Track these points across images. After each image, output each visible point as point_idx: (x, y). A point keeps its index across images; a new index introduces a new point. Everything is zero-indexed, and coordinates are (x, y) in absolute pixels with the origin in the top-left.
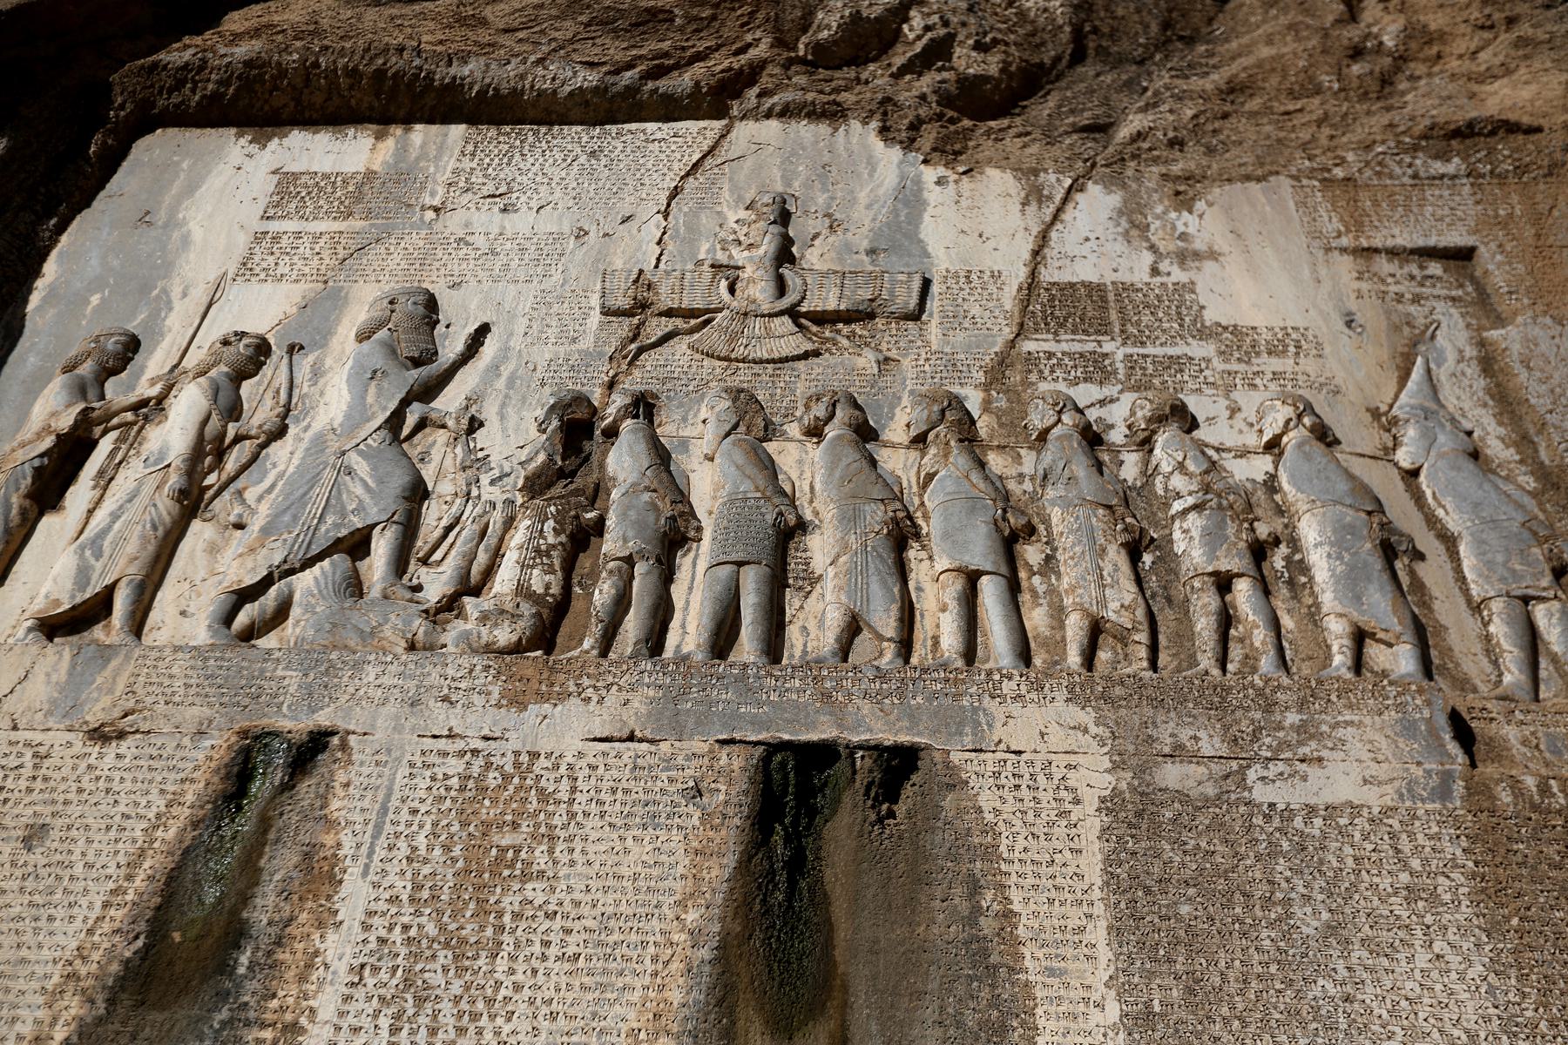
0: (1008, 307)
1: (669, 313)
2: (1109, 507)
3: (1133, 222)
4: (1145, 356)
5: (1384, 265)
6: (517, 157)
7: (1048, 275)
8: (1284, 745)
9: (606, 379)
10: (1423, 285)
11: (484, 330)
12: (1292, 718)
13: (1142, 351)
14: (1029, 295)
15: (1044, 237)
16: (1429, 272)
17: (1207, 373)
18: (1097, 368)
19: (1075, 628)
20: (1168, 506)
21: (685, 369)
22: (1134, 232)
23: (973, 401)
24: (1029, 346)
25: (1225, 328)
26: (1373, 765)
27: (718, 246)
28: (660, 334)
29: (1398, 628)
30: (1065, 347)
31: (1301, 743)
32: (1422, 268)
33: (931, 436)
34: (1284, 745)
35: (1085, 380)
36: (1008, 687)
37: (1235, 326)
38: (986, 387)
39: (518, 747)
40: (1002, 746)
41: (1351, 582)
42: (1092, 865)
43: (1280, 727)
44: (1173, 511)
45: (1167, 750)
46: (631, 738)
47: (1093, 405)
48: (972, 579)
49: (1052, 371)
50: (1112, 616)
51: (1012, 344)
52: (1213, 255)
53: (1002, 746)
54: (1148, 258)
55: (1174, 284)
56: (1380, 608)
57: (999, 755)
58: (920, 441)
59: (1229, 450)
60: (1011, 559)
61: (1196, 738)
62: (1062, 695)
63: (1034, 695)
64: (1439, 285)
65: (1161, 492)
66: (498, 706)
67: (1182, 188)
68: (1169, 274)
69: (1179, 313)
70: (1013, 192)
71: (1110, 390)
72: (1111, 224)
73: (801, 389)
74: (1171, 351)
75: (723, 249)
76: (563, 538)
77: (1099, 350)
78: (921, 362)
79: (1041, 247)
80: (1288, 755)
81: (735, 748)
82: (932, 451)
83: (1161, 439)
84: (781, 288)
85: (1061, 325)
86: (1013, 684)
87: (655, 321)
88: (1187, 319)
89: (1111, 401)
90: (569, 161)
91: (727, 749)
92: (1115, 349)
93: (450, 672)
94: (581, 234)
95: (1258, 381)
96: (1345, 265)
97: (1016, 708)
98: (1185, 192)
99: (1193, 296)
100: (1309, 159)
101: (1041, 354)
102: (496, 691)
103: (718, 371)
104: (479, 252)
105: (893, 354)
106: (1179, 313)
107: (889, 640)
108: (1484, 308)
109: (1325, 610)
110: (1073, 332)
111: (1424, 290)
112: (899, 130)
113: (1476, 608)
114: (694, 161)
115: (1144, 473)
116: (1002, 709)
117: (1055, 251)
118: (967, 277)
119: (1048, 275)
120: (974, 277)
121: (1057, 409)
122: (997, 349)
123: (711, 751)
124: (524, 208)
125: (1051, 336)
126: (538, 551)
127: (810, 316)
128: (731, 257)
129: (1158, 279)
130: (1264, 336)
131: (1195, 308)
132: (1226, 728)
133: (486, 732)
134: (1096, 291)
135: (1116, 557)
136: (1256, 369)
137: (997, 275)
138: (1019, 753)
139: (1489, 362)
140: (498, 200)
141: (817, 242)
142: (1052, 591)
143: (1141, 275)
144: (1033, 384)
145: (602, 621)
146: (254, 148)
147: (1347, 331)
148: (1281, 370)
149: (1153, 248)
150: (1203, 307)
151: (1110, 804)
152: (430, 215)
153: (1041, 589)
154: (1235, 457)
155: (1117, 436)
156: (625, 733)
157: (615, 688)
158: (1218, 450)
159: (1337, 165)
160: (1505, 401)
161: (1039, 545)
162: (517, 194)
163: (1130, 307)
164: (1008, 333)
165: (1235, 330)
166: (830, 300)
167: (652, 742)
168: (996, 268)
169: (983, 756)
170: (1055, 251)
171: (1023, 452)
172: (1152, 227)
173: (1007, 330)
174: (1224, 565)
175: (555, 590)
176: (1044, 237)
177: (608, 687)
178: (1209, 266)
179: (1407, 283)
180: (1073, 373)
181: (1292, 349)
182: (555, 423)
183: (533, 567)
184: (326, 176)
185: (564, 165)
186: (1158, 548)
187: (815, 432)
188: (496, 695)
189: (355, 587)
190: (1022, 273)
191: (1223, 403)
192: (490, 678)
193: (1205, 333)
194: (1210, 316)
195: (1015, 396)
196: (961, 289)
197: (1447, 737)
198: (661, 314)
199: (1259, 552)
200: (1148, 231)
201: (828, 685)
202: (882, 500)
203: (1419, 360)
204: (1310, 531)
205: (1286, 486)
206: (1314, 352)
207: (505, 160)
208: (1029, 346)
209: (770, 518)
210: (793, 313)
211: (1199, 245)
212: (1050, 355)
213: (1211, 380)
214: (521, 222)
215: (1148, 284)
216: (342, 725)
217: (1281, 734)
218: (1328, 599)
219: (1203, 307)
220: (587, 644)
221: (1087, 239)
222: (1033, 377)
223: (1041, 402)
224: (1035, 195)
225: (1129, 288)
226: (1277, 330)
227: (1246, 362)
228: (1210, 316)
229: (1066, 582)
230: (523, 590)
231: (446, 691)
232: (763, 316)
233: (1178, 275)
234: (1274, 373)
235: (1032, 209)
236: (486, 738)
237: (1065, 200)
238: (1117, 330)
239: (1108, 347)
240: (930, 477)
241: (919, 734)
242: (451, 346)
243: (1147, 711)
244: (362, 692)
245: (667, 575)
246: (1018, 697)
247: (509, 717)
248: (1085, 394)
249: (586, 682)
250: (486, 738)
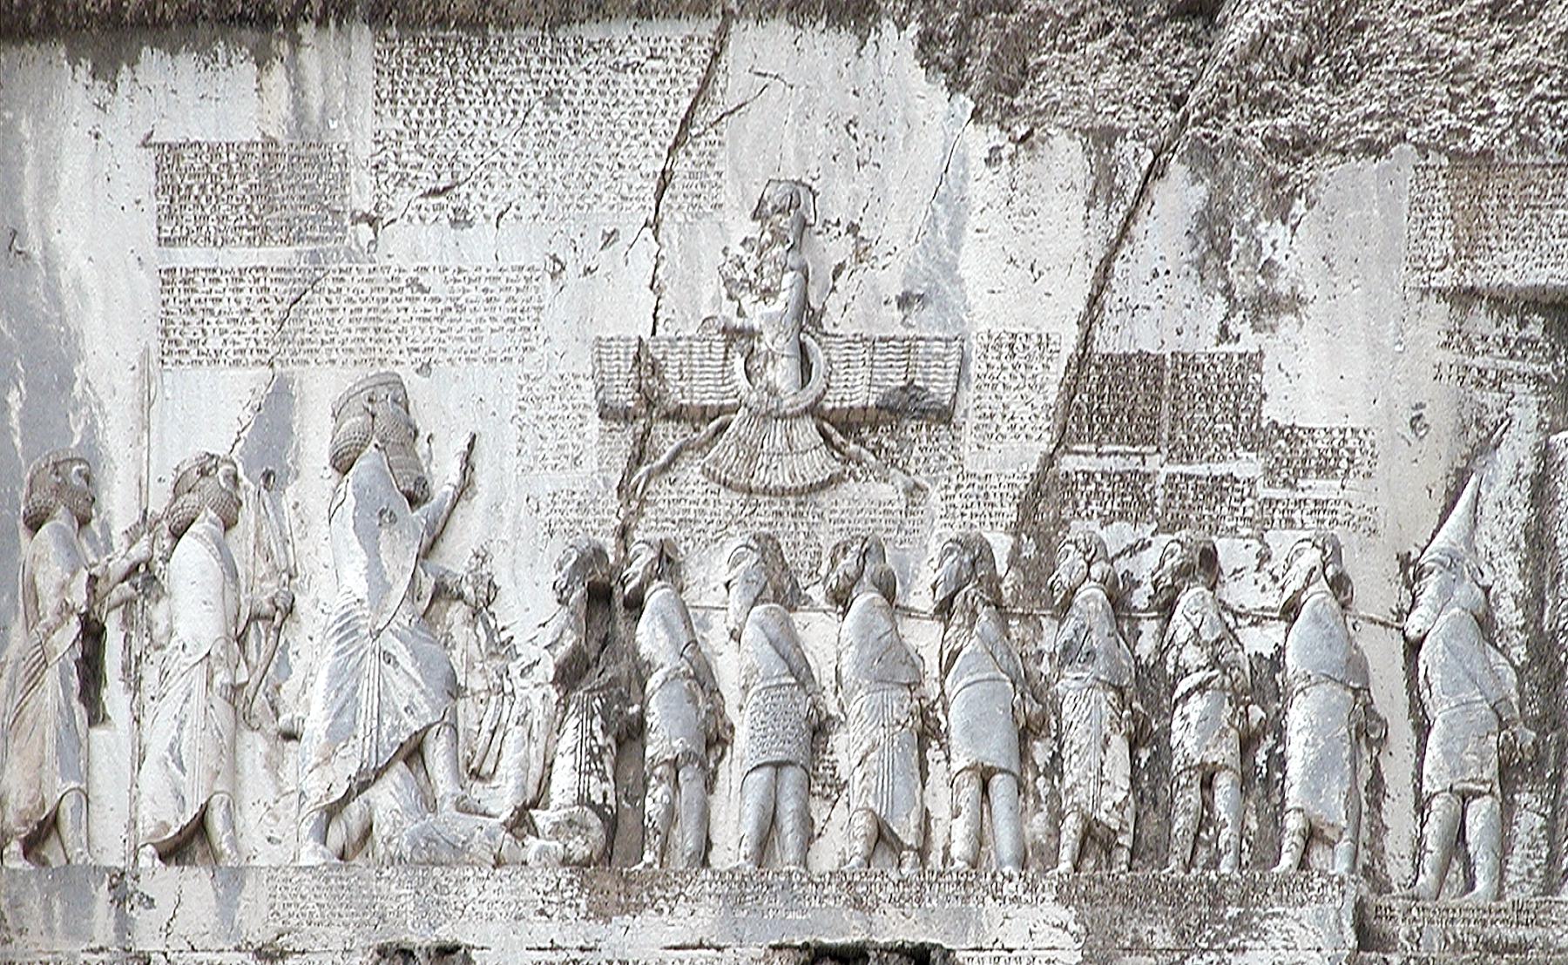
0: (1052, 400)
1: (677, 415)
2: (1120, 691)
4: (1188, 477)
5: (1482, 321)
6: (453, 108)
7: (1100, 347)
8: (1220, 936)
9: (618, 522)
10: (1512, 356)
12: (1233, 911)
13: (1186, 469)
14: (1076, 378)
15: (1105, 271)
16: (1525, 333)
17: (1248, 502)
19: (1071, 824)
20: (1174, 688)
21: (701, 506)
22: (1212, 261)
23: (1001, 545)
24: (1069, 463)
25: (1281, 431)
26: (1283, 951)
27: (724, 292)
28: (670, 450)
29: (1344, 823)
30: (1108, 463)
31: (1233, 935)
32: (1522, 324)
33: (958, 600)
34: (1220, 936)
35: (1122, 516)
36: (1008, 888)
37: (1293, 427)
38: (1016, 530)
39: (610, 957)
40: (998, 945)
43: (1221, 921)
44: (1177, 694)
45: (1127, 944)
46: (701, 946)
47: (1123, 552)
48: (985, 778)
49: (1088, 503)
50: (1103, 816)
51: (1050, 459)
53: (998, 945)
54: (1220, 305)
55: (1240, 356)
56: (1334, 809)
57: (995, 953)
58: (944, 609)
59: (1247, 615)
60: (1024, 755)
61: (1152, 933)
62: (1050, 896)
63: (1028, 896)
64: (1530, 355)
65: (1170, 670)
66: (586, 918)
67: (1282, 169)
68: (1238, 339)
69: (1236, 406)
70: (1079, 178)
71: (1146, 531)
72: (1186, 242)
73: (827, 539)
74: (1219, 469)
75: (730, 297)
76: (610, 740)
77: (1141, 469)
78: (951, 492)
79: (1101, 289)
80: (1221, 945)
81: (786, 952)
82: (957, 619)
83: (1185, 600)
85: (1107, 428)
86: (1012, 886)
87: (660, 428)
88: (1243, 416)
89: (1143, 548)
90: (521, 115)
91: (778, 954)
92: (1159, 466)
93: (541, 886)
94: (558, 267)
95: (1297, 516)
96: (1439, 311)
97: (1011, 909)
98: (1283, 180)
99: (1258, 376)
100: (1453, 109)
101: (1080, 476)
102: (582, 902)
103: (737, 508)
104: (441, 306)
105: (921, 480)
106: (1236, 406)
107: (910, 848)
109: (1289, 805)
110: (1118, 442)
111: (1511, 363)
112: (942, 40)
114: (683, 113)
115: (1158, 647)
116: (1002, 910)
117: (1116, 297)
118: (1011, 346)
120: (1018, 344)
121: (1088, 557)
122: (1033, 469)
123: (766, 956)
124: (480, 220)
125: (1093, 448)
126: (590, 752)
127: (833, 417)
128: (740, 313)
129: (1225, 348)
130: (1319, 444)
131: (1256, 397)
132: (1178, 923)
133: (581, 943)
135: (1119, 745)
136: (1300, 495)
137: (1044, 342)
138: (1010, 951)
140: (442, 200)
141: (841, 283)
142: (1055, 795)
143: (1206, 344)
144: (1066, 522)
145: (659, 833)
146: (100, 89)
147: (1409, 434)
148: (1324, 498)
149: (1228, 291)
150: (1264, 396)
152: (365, 230)
153: (1044, 792)
154: (1252, 624)
156: (695, 941)
157: (682, 898)
158: (1236, 615)
159: (1480, 121)
161: (1048, 740)
162: (464, 189)
163: (1185, 398)
164: (1045, 446)
165: (1290, 434)
167: (719, 949)
168: (1044, 331)
169: (981, 954)
170: (1116, 297)
171: (1045, 622)
172: (1235, 247)
173: (1047, 436)
174: (1213, 756)
175: (611, 801)
176: (1105, 271)
177: (676, 898)
179: (1496, 352)
180: (1109, 506)
181: (1344, 464)
182: (579, 592)
183: (590, 773)
184: (215, 152)
185: (516, 123)
186: (1157, 741)
187: (841, 599)
188: (583, 907)
191: (1256, 546)
192: (576, 891)
193: (1257, 438)
194: (1270, 411)
195: (1048, 547)
196: (1003, 368)
197: (1347, 924)
198: (667, 417)
199: (1248, 743)
200: (1228, 258)
201: (860, 890)
202: (909, 686)
203: (1474, 479)
204: (1298, 717)
205: (1291, 660)
206: (1366, 468)
207: (438, 114)
208: (1069, 463)
209: (804, 709)
210: (814, 410)
211: (1282, 287)
212: (1089, 476)
213: (1249, 513)
214: (480, 243)
215: (1211, 356)
216: (463, 941)
217: (1219, 927)
218: (1294, 796)
219: (1264, 396)
220: (648, 857)
221: (1156, 275)
222: (1067, 513)
223: (1071, 547)
224: (1104, 186)
225: (1187, 362)
226: (1336, 433)
227: (1293, 487)
228: (1270, 411)
229: (1069, 781)
230: (583, 800)
231: (541, 905)
232: (784, 417)
233: (1249, 341)
234: (1316, 502)
235: (1097, 214)
236: (582, 949)
237: (1142, 192)
238: (1165, 436)
239: (1153, 464)
240: (954, 655)
241: (934, 936)
242: (444, 476)
243: (1118, 909)
244: (469, 908)
246: (1015, 899)
247: (596, 929)
248: (1118, 535)
249: (658, 893)
250: (582, 949)
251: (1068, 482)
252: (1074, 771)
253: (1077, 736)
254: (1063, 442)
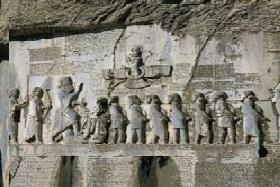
3: (221, 48)
11: (82, 84)
18: (208, 85)
41: (249, 129)
48: (178, 129)
52: (240, 56)
54: (224, 58)
84: (140, 72)
134: (210, 67)
143: (221, 62)
151: (197, 164)
165: (240, 74)
174: (226, 126)
178: (238, 59)
190: (193, 64)
193: (234, 76)
210: (143, 78)
214: (84, 58)
224: (198, 42)
225: (217, 66)
228: (236, 72)
233: (230, 61)
242: (77, 89)
245: (125, 131)
252: (197, 128)
254: (193, 77)
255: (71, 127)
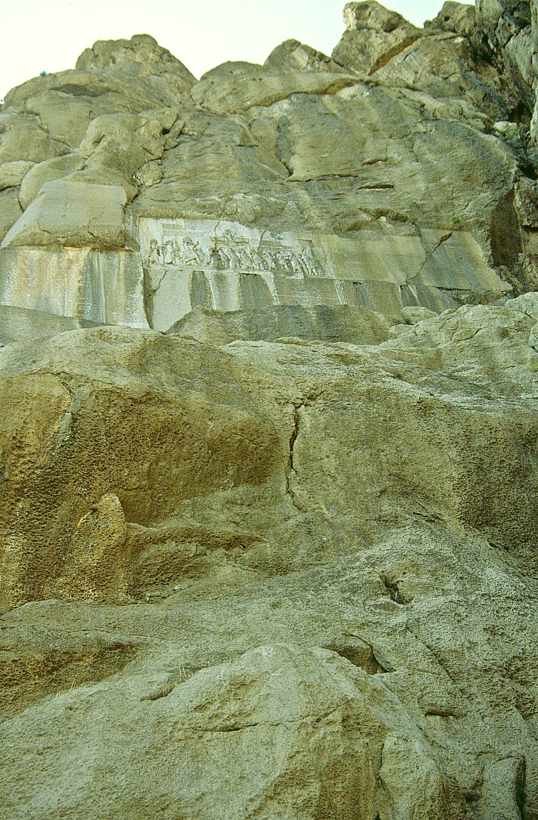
19: (270, 268)
42: (273, 281)
108: (312, 246)
113: (308, 269)
119: (263, 240)
135: (273, 263)
139: (312, 251)
155: (272, 254)
160: (313, 254)
164: (259, 245)
166: (238, 241)
189: (197, 262)
190: (260, 239)
199: (287, 264)
233: (278, 241)
242: (195, 243)
251: (262, 248)
253: (268, 261)
255: (195, 259)
